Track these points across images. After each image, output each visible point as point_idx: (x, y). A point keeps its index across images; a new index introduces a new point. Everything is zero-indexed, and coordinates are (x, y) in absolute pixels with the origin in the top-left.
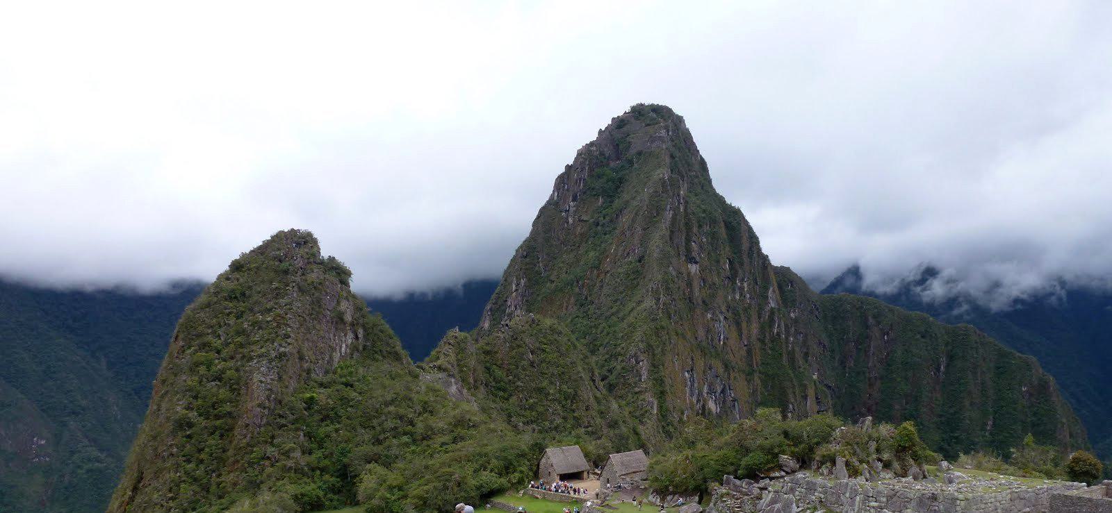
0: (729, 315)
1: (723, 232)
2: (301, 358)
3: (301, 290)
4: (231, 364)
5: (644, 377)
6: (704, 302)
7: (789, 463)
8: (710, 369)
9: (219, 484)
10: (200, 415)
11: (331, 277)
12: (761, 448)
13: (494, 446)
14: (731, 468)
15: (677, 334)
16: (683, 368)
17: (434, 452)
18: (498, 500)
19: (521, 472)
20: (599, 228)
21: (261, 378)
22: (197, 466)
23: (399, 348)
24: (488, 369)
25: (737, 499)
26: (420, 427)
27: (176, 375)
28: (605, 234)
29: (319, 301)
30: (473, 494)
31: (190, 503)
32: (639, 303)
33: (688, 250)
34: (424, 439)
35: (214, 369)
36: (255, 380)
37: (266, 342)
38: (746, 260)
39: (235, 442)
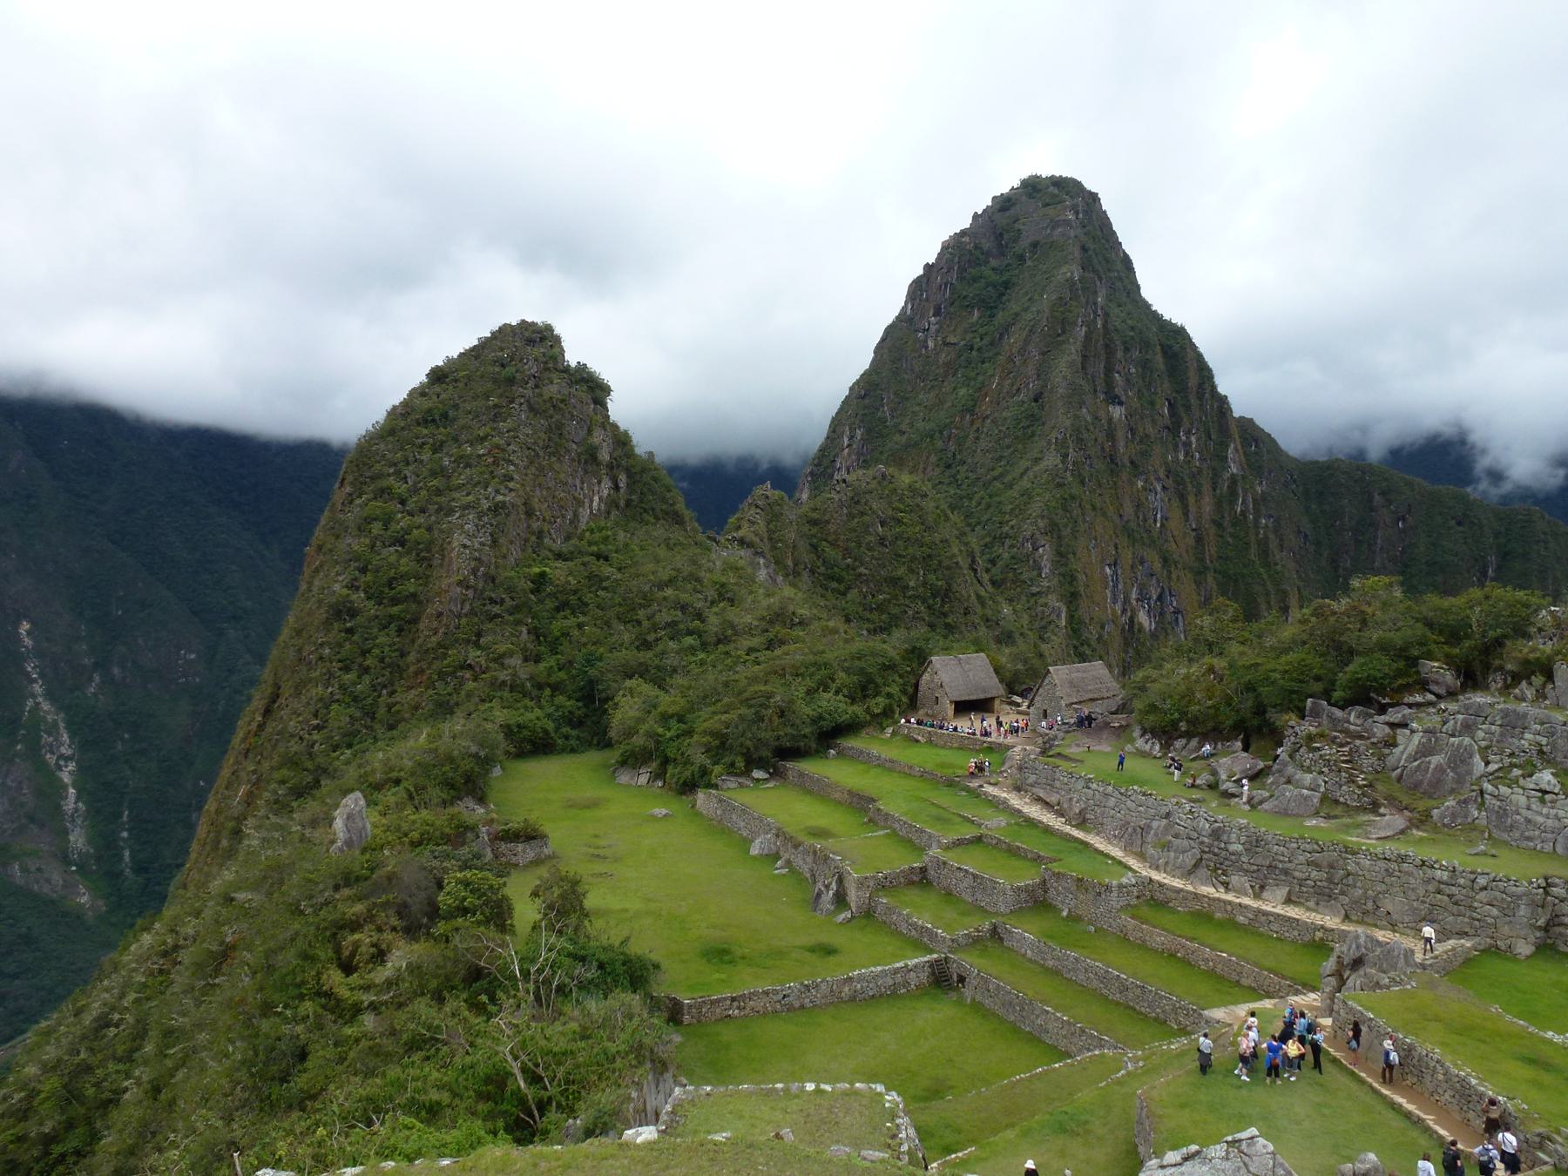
1: (1159, 361)
2: (529, 513)
3: (531, 408)
4: (420, 519)
5: (1045, 571)
6: (1132, 462)
7: (1444, 676)
8: (1142, 563)
11: (581, 392)
12: (1383, 647)
13: (836, 651)
14: (1318, 687)
15: (1094, 508)
16: (1103, 561)
17: (735, 664)
19: (889, 695)
20: (974, 353)
21: (463, 540)
22: (359, 677)
23: (681, 506)
24: (814, 547)
25: (1342, 745)
26: (713, 622)
27: (338, 537)
29: (560, 426)
30: (807, 731)
32: (1037, 460)
33: (1110, 385)
34: (719, 642)
35: (393, 527)
36: (455, 544)
38: (1194, 401)
39: (420, 641)
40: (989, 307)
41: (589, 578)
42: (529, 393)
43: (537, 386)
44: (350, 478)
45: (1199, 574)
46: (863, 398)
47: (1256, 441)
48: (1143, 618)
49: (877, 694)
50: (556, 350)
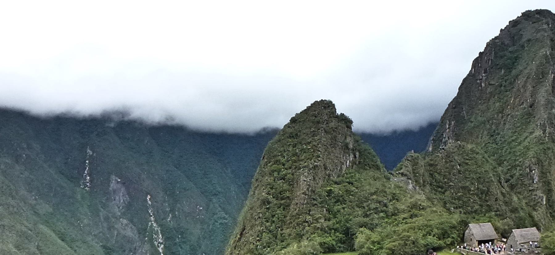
2: (326, 168)
3: (325, 132)
9: (281, 234)
10: (274, 198)
13: (435, 221)
17: (399, 223)
19: (453, 238)
20: (502, 88)
22: (271, 224)
24: (431, 175)
26: (391, 208)
28: (507, 91)
29: (335, 137)
30: (422, 249)
32: (531, 133)
34: (393, 215)
35: (281, 173)
40: (509, 68)
41: (346, 191)
42: (324, 126)
43: (327, 123)
44: (266, 157)
46: (454, 108)
49: (449, 237)
50: (334, 110)
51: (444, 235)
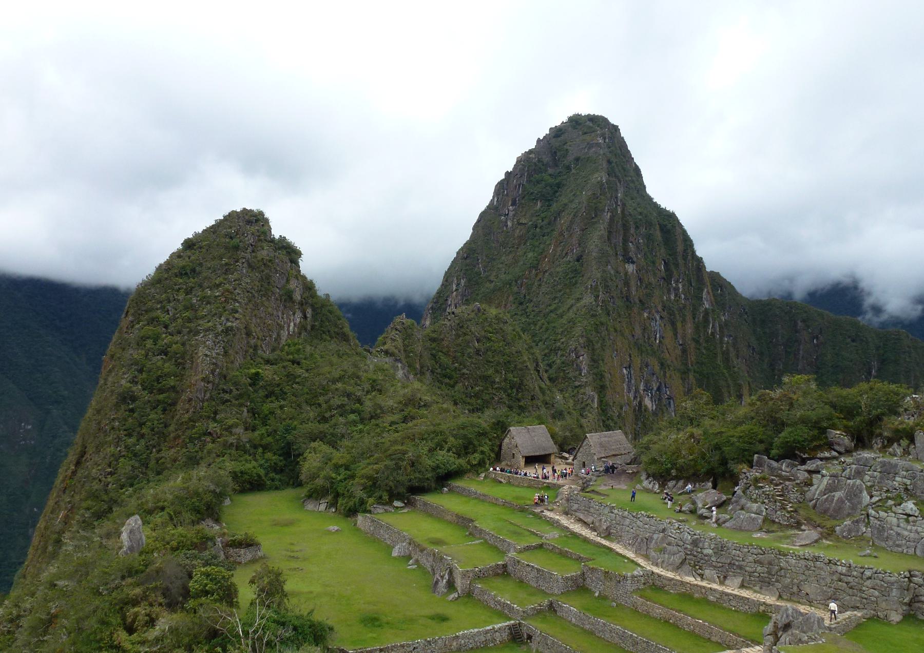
0: (665, 314)
1: (658, 235)
2: (248, 334)
3: (250, 266)
4: (177, 338)
5: (584, 371)
6: (640, 301)
8: (647, 366)
9: (157, 460)
10: (144, 389)
11: (282, 255)
15: (616, 331)
16: (621, 365)
17: (382, 432)
18: (458, 483)
19: (482, 452)
20: (538, 230)
21: (206, 351)
22: (138, 440)
24: (434, 356)
26: (368, 405)
27: (124, 349)
29: (268, 277)
30: (429, 475)
31: (128, 478)
32: (578, 300)
33: (626, 250)
34: (372, 417)
35: (160, 343)
37: (213, 316)
38: (681, 261)
39: (178, 417)
40: (548, 200)
41: (287, 376)
42: (248, 255)
43: (253, 251)
44: (132, 311)
45: (684, 373)
47: (721, 287)
48: (647, 402)
49: (475, 451)
50: (266, 228)
51: (466, 448)
